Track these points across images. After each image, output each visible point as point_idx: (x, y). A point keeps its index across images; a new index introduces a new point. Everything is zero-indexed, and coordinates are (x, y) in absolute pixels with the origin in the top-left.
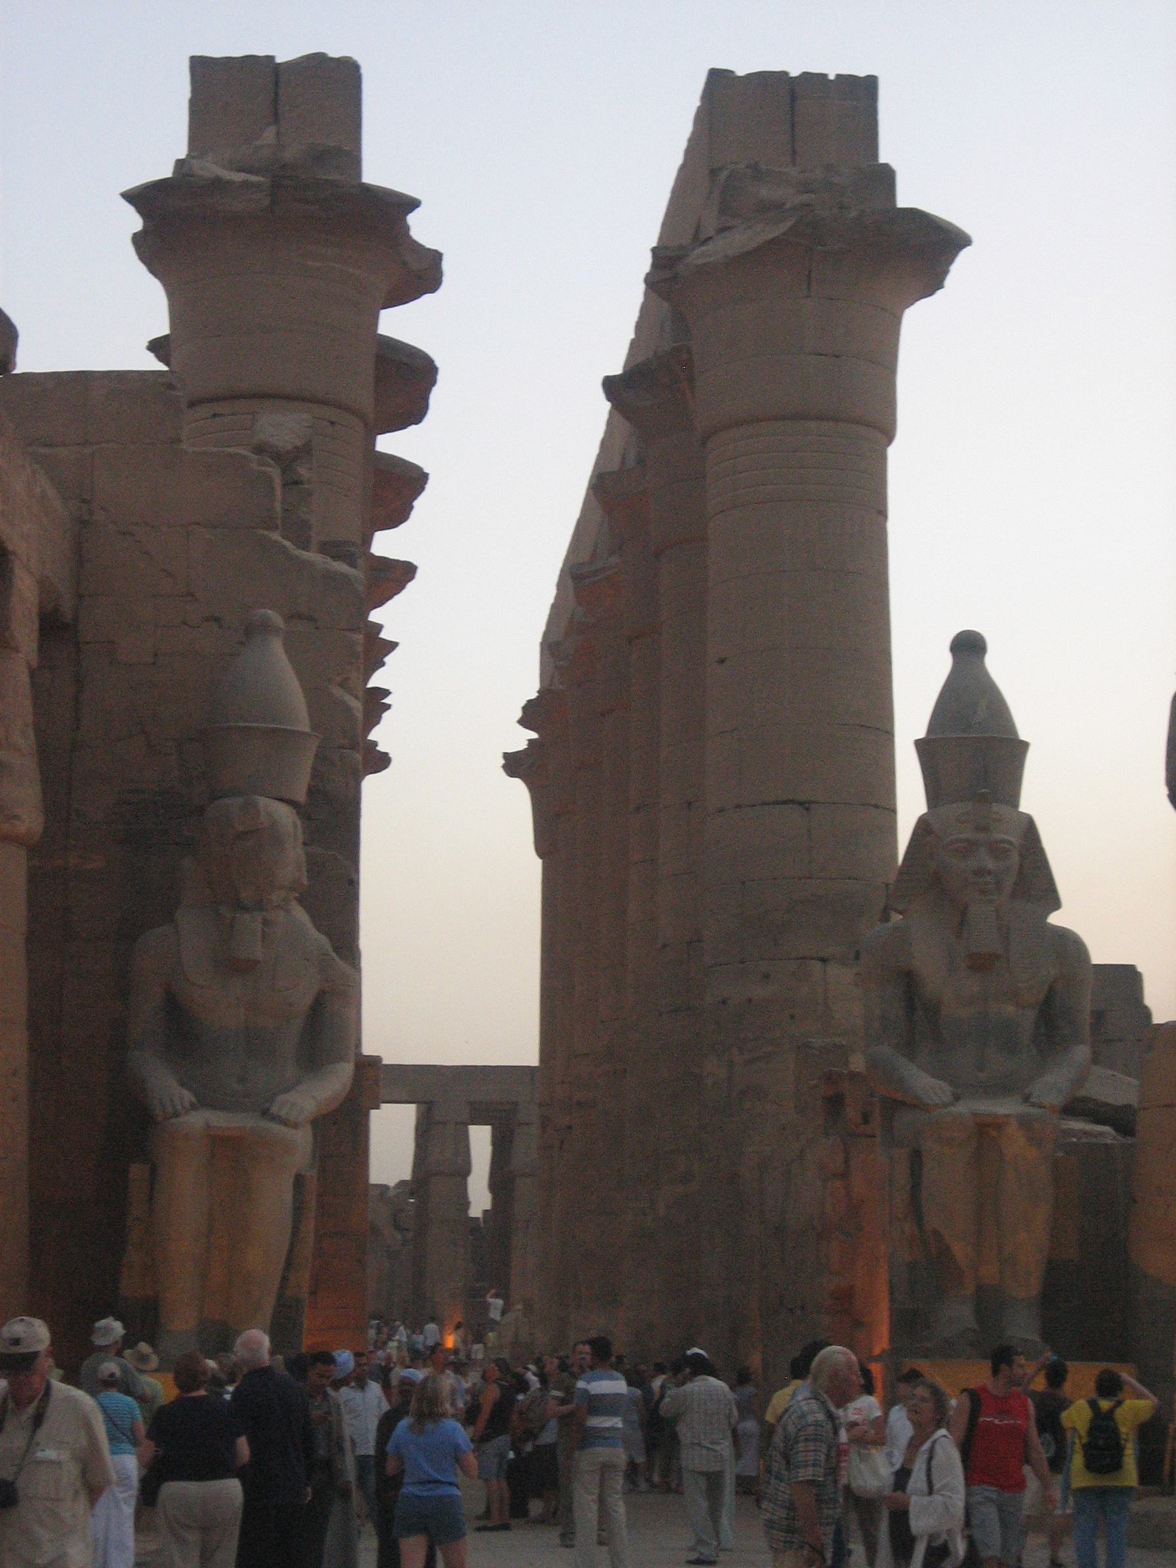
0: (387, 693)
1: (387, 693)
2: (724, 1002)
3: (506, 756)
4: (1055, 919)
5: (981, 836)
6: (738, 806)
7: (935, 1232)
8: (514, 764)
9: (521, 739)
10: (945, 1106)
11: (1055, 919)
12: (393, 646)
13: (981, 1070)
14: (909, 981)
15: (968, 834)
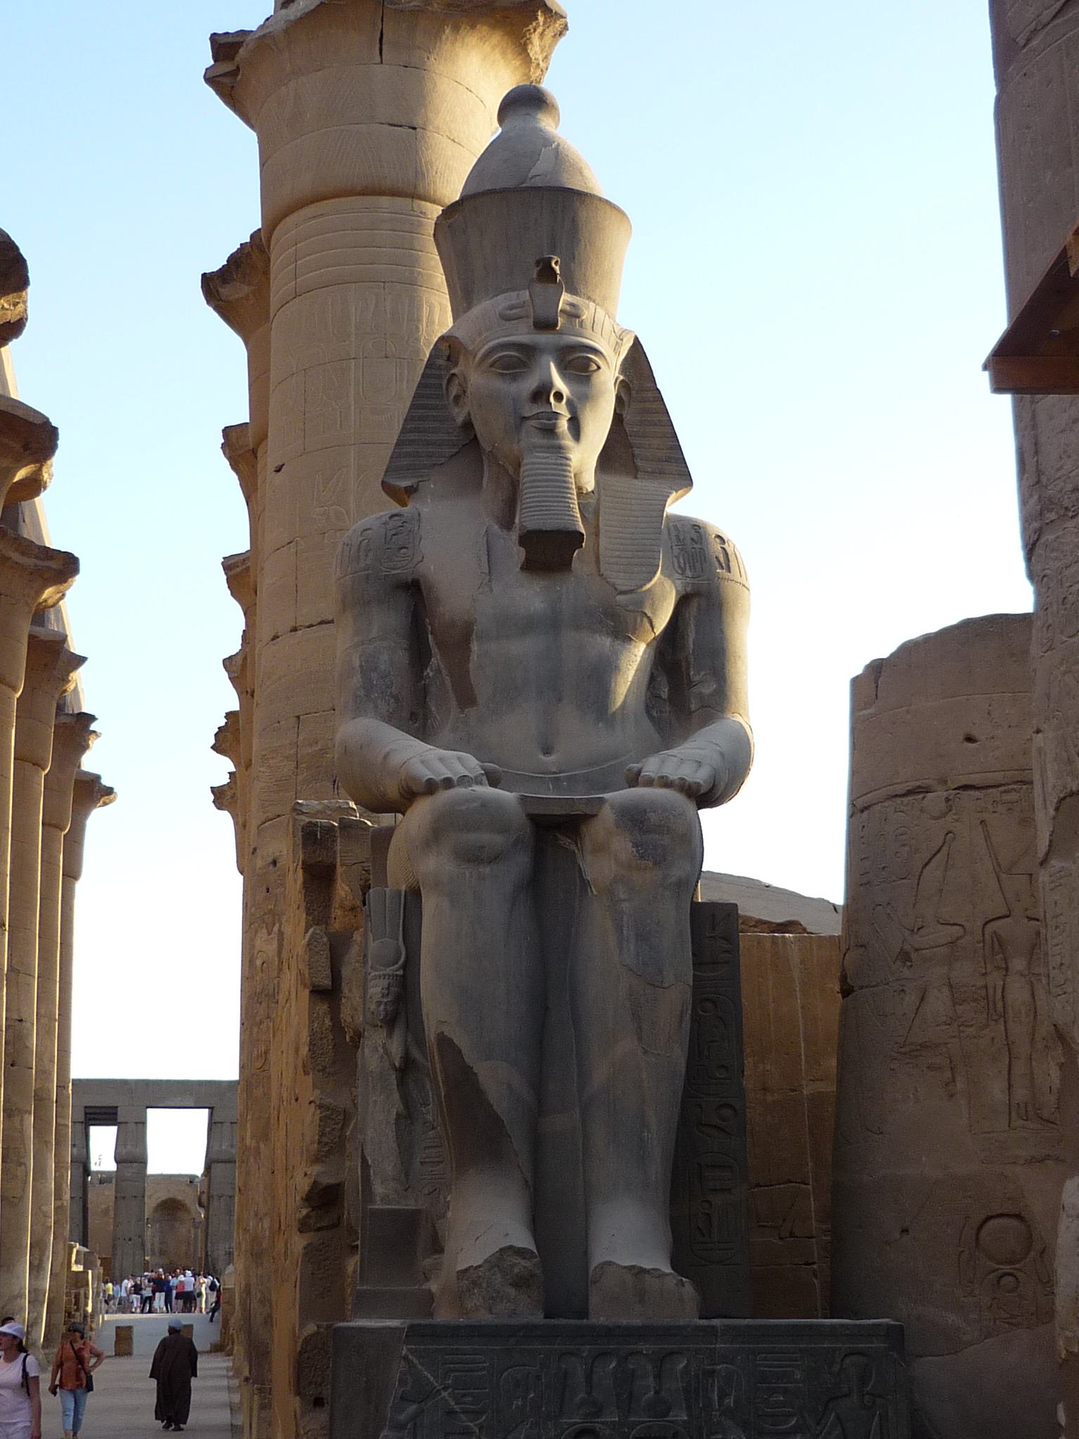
0: (92, 718)
1: (92, 718)
2: (274, 863)
3: (214, 790)
4: (679, 506)
5: (543, 338)
6: (295, 629)
7: (445, 1042)
8: (221, 797)
9: (221, 769)
10: (464, 781)
11: (679, 506)
12: (82, 660)
13: (547, 751)
14: (414, 592)
15: (524, 335)
